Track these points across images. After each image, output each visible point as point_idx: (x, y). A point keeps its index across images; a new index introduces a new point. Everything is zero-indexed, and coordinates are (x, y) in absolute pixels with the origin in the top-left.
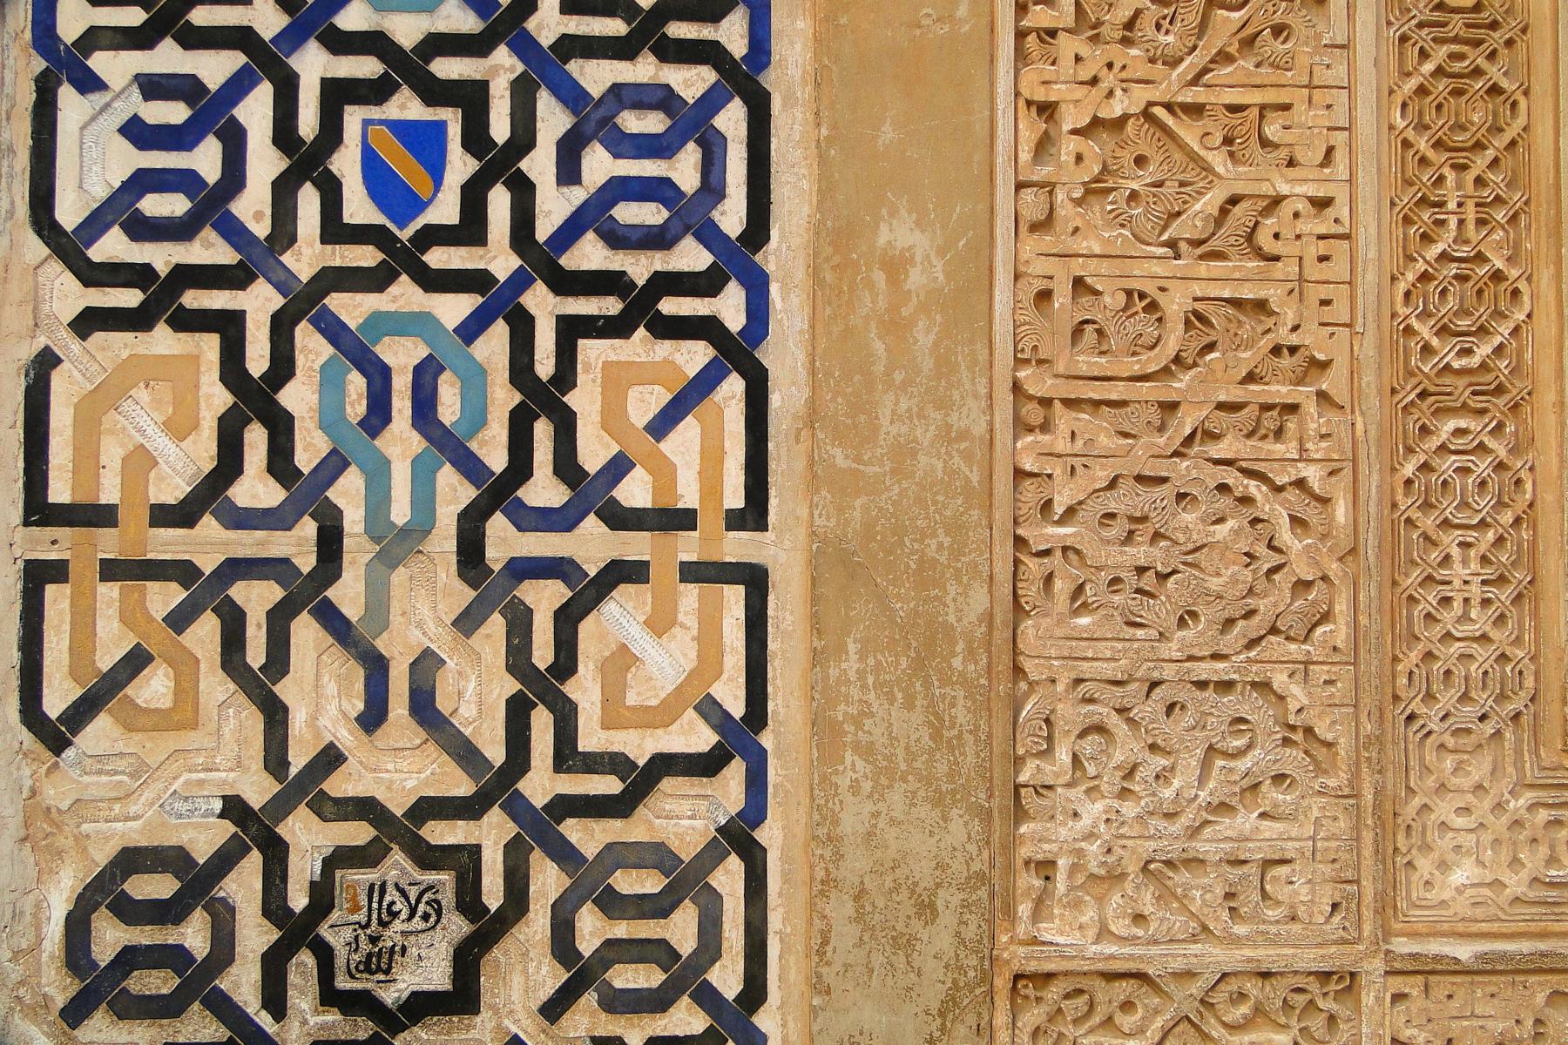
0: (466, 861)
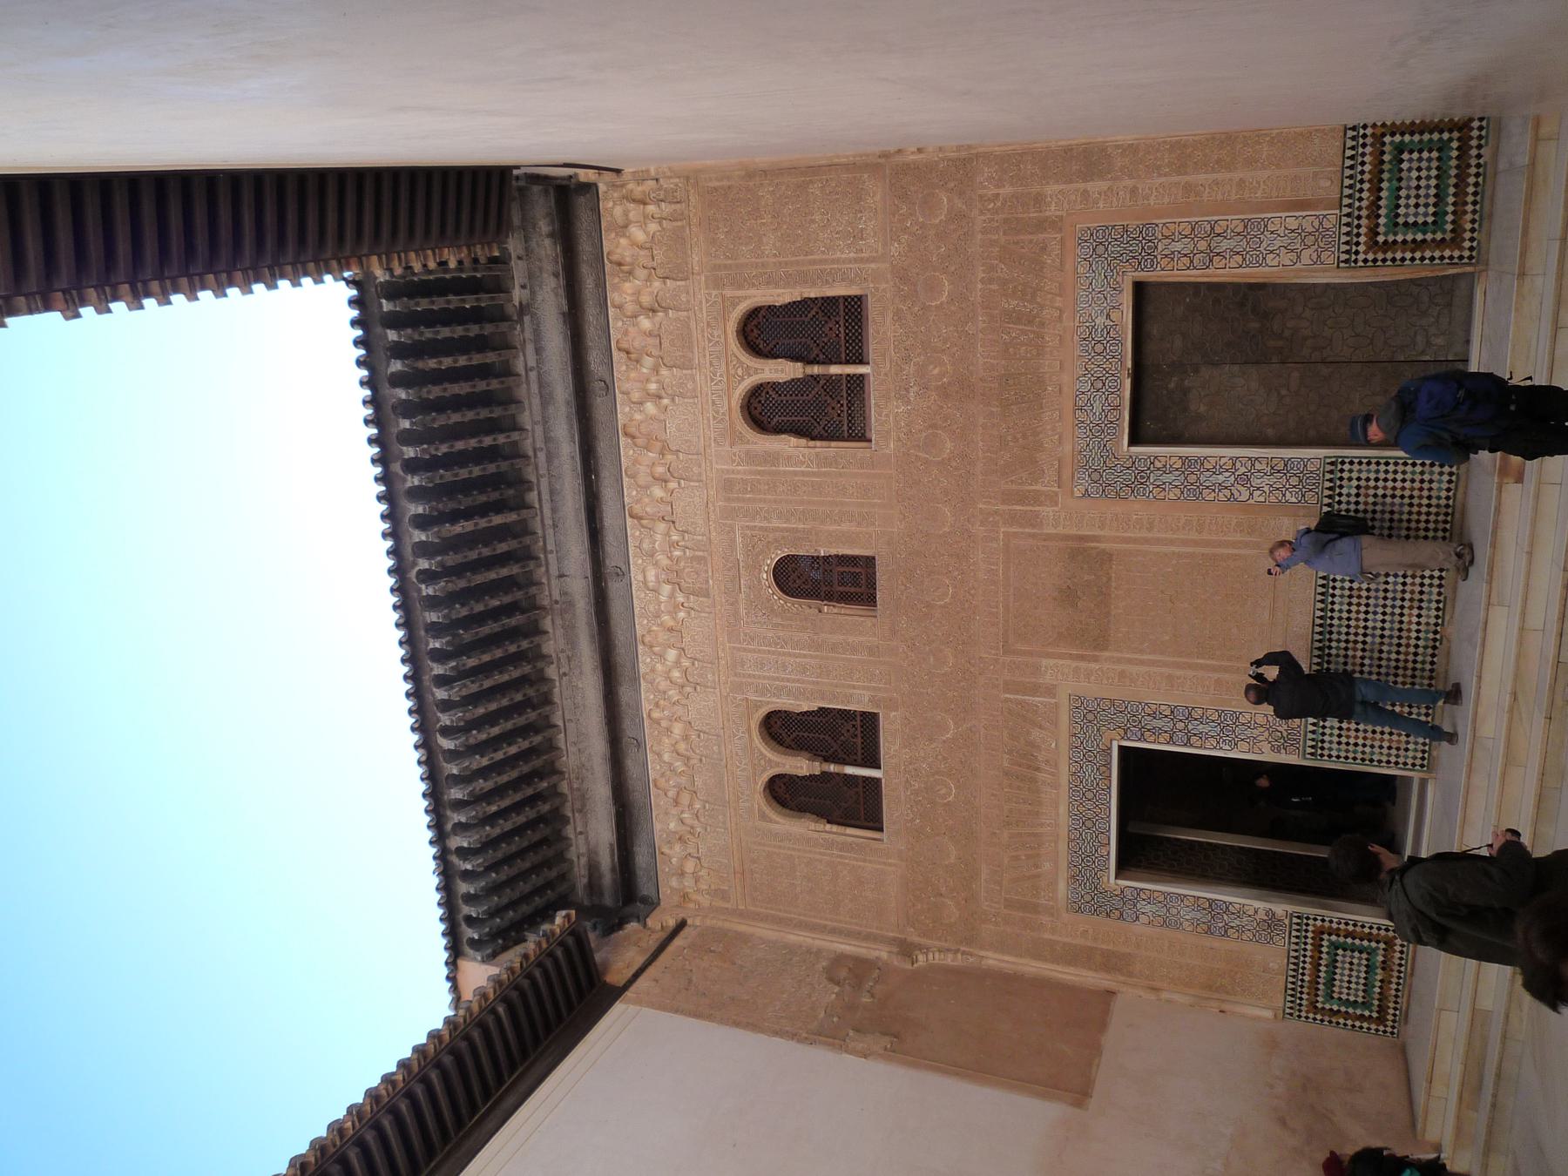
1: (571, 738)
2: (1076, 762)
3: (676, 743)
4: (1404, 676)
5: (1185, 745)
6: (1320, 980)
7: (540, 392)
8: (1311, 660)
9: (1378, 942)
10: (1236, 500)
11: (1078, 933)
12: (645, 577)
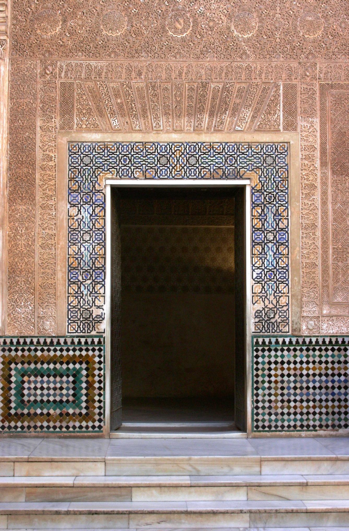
0: (274, 311)
2: (224, 149)
4: (333, 407)
5: (253, 241)
6: (39, 366)
8: (340, 336)
9: (87, 408)
11: (47, 152)
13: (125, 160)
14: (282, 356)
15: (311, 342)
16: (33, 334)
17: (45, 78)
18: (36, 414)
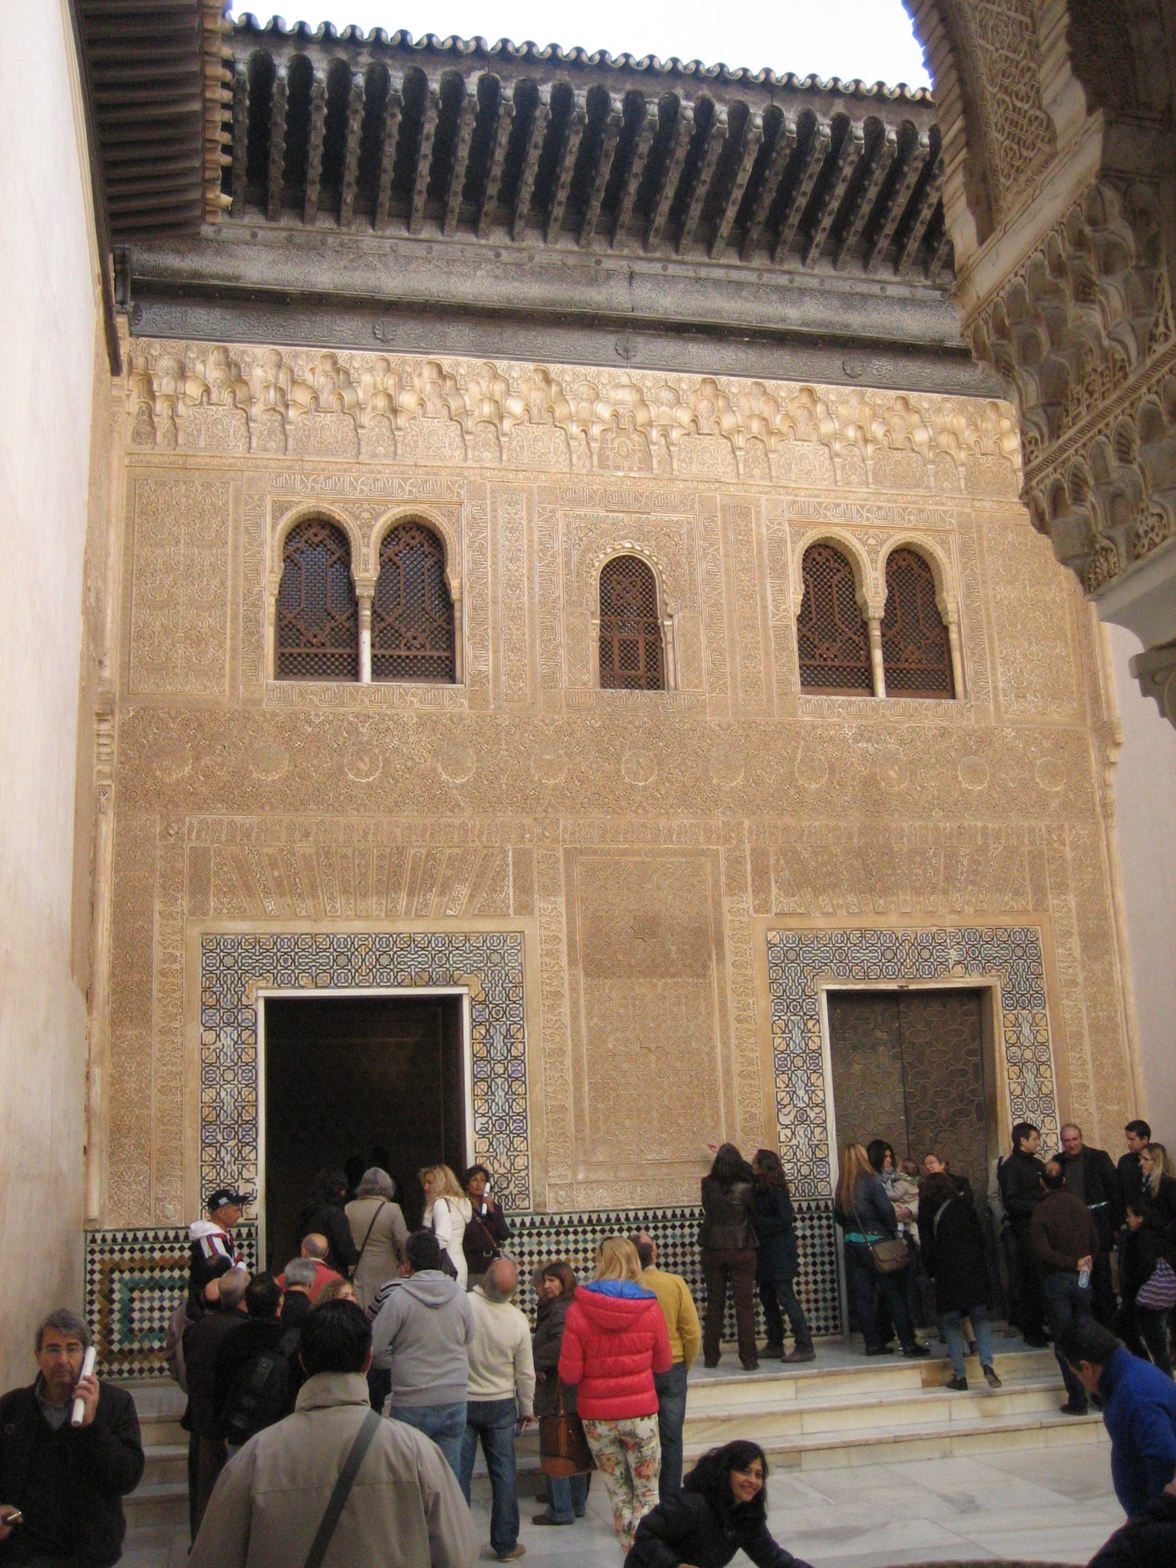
1: (404, 248)
3: (389, 396)
5: (475, 1076)
6: (157, 1274)
7: (857, 294)
10: (779, 1110)
11: (170, 950)
12: (624, 386)
13: (285, 961)
14: (521, 1244)
15: (561, 1222)
16: (148, 1225)
17: (167, 840)
18: (151, 1350)
